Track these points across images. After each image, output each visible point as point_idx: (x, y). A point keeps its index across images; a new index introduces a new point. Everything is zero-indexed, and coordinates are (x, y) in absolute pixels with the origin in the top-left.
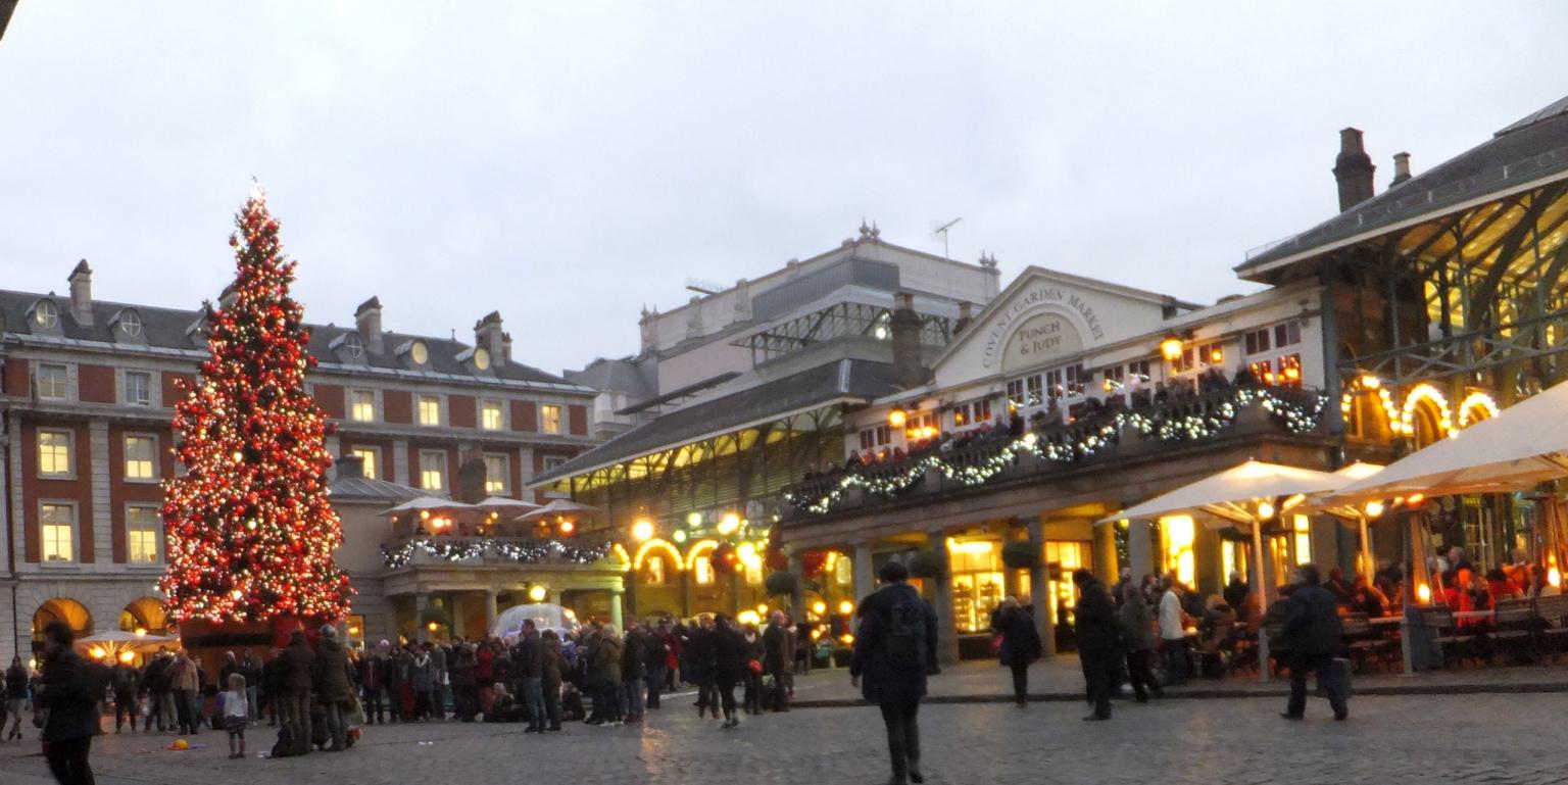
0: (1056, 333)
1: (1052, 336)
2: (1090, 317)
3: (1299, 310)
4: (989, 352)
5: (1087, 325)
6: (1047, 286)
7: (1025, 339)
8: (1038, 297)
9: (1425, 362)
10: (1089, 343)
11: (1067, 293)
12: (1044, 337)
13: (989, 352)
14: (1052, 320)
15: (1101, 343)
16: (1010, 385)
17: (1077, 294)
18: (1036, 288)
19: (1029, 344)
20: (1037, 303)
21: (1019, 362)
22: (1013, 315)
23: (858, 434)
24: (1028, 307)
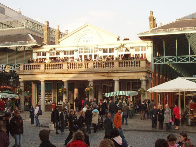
3: (147, 45)
9: (169, 60)
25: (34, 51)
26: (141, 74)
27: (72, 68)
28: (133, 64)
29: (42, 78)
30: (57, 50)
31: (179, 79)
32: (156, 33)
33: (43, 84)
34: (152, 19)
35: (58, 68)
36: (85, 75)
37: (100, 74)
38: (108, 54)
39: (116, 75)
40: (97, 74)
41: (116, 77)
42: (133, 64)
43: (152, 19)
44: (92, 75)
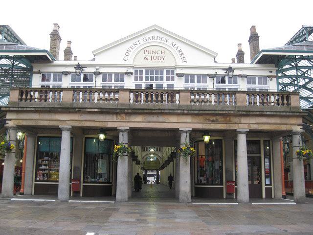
0: (163, 55)
1: (161, 55)
2: (181, 53)
4: (127, 54)
5: (179, 56)
6: (161, 35)
7: (147, 53)
8: (156, 38)
10: (180, 63)
11: (171, 41)
12: (157, 55)
13: (127, 54)
14: (163, 50)
15: (185, 64)
16: (136, 71)
17: (175, 42)
18: (156, 34)
19: (149, 56)
20: (154, 40)
21: (141, 62)
23: (41, 75)
24: (149, 41)
26: (293, 121)
34: (254, 38)
36: (173, 119)
39: (244, 120)
43: (254, 38)
44: (189, 119)
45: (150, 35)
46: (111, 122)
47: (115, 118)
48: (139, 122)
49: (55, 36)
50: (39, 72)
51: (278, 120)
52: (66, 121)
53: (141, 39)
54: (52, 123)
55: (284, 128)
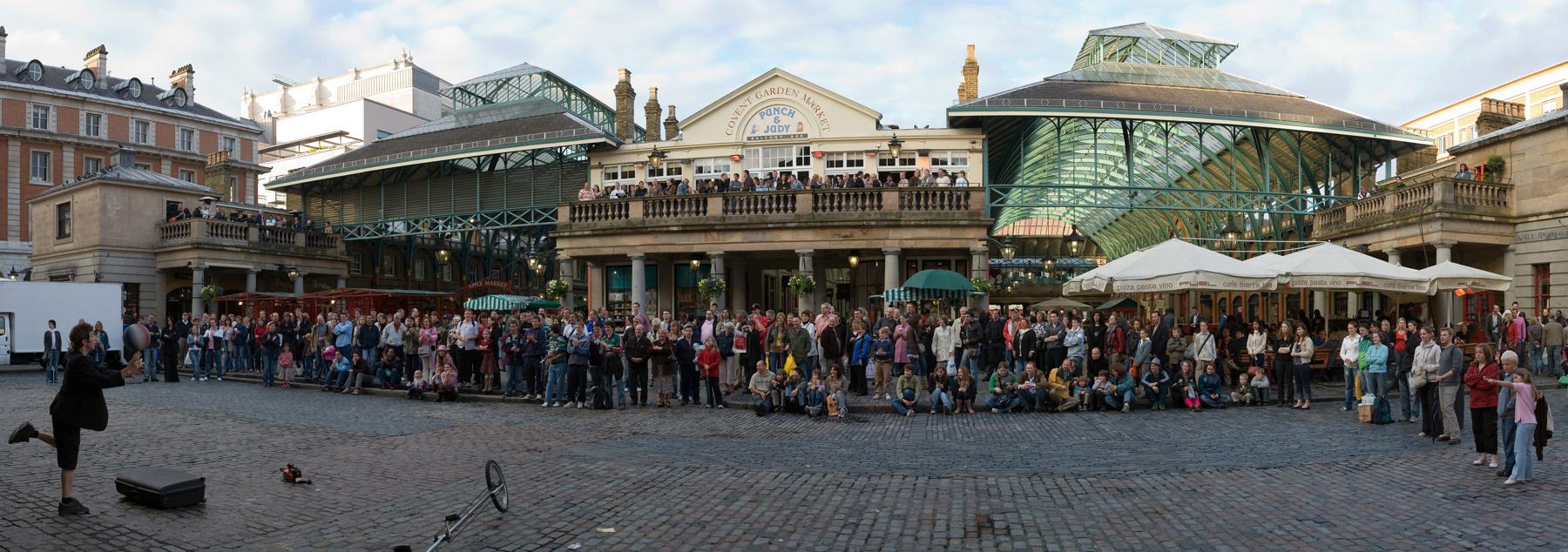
15: (826, 135)
22: (755, 102)
25: (593, 163)
26: (971, 233)
27: (926, 207)
28: (946, 202)
29: (635, 246)
30: (671, 156)
31: (1174, 243)
32: (1021, 107)
33: (637, 268)
35: (778, 210)
36: (786, 236)
37: (837, 231)
38: (845, 171)
39: (892, 233)
40: (828, 232)
41: (893, 241)
42: (946, 202)
44: (809, 235)
45: (767, 87)
46: (696, 243)
47: (701, 238)
48: (738, 242)
49: (625, 92)
50: (600, 166)
51: (946, 233)
52: (635, 246)
53: (752, 95)
54: (617, 251)
55: (956, 245)
